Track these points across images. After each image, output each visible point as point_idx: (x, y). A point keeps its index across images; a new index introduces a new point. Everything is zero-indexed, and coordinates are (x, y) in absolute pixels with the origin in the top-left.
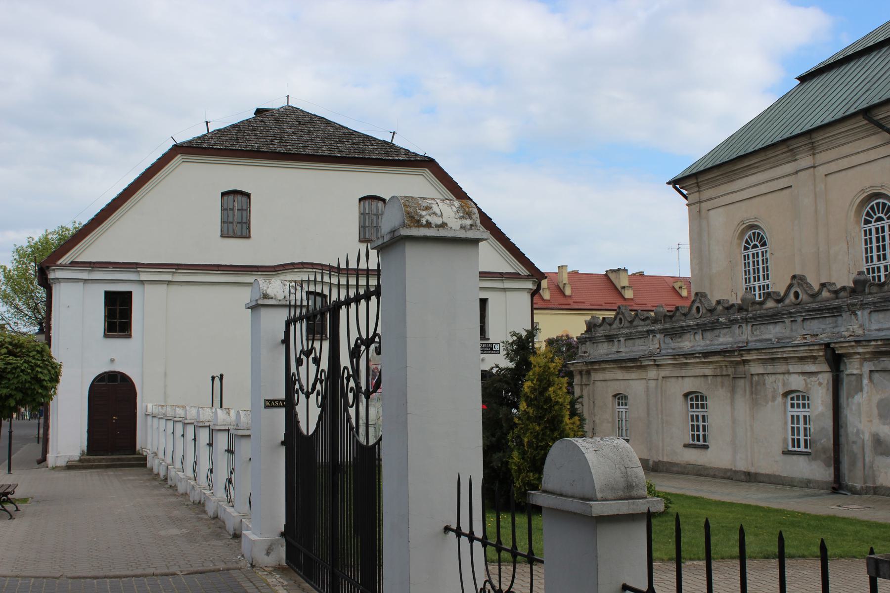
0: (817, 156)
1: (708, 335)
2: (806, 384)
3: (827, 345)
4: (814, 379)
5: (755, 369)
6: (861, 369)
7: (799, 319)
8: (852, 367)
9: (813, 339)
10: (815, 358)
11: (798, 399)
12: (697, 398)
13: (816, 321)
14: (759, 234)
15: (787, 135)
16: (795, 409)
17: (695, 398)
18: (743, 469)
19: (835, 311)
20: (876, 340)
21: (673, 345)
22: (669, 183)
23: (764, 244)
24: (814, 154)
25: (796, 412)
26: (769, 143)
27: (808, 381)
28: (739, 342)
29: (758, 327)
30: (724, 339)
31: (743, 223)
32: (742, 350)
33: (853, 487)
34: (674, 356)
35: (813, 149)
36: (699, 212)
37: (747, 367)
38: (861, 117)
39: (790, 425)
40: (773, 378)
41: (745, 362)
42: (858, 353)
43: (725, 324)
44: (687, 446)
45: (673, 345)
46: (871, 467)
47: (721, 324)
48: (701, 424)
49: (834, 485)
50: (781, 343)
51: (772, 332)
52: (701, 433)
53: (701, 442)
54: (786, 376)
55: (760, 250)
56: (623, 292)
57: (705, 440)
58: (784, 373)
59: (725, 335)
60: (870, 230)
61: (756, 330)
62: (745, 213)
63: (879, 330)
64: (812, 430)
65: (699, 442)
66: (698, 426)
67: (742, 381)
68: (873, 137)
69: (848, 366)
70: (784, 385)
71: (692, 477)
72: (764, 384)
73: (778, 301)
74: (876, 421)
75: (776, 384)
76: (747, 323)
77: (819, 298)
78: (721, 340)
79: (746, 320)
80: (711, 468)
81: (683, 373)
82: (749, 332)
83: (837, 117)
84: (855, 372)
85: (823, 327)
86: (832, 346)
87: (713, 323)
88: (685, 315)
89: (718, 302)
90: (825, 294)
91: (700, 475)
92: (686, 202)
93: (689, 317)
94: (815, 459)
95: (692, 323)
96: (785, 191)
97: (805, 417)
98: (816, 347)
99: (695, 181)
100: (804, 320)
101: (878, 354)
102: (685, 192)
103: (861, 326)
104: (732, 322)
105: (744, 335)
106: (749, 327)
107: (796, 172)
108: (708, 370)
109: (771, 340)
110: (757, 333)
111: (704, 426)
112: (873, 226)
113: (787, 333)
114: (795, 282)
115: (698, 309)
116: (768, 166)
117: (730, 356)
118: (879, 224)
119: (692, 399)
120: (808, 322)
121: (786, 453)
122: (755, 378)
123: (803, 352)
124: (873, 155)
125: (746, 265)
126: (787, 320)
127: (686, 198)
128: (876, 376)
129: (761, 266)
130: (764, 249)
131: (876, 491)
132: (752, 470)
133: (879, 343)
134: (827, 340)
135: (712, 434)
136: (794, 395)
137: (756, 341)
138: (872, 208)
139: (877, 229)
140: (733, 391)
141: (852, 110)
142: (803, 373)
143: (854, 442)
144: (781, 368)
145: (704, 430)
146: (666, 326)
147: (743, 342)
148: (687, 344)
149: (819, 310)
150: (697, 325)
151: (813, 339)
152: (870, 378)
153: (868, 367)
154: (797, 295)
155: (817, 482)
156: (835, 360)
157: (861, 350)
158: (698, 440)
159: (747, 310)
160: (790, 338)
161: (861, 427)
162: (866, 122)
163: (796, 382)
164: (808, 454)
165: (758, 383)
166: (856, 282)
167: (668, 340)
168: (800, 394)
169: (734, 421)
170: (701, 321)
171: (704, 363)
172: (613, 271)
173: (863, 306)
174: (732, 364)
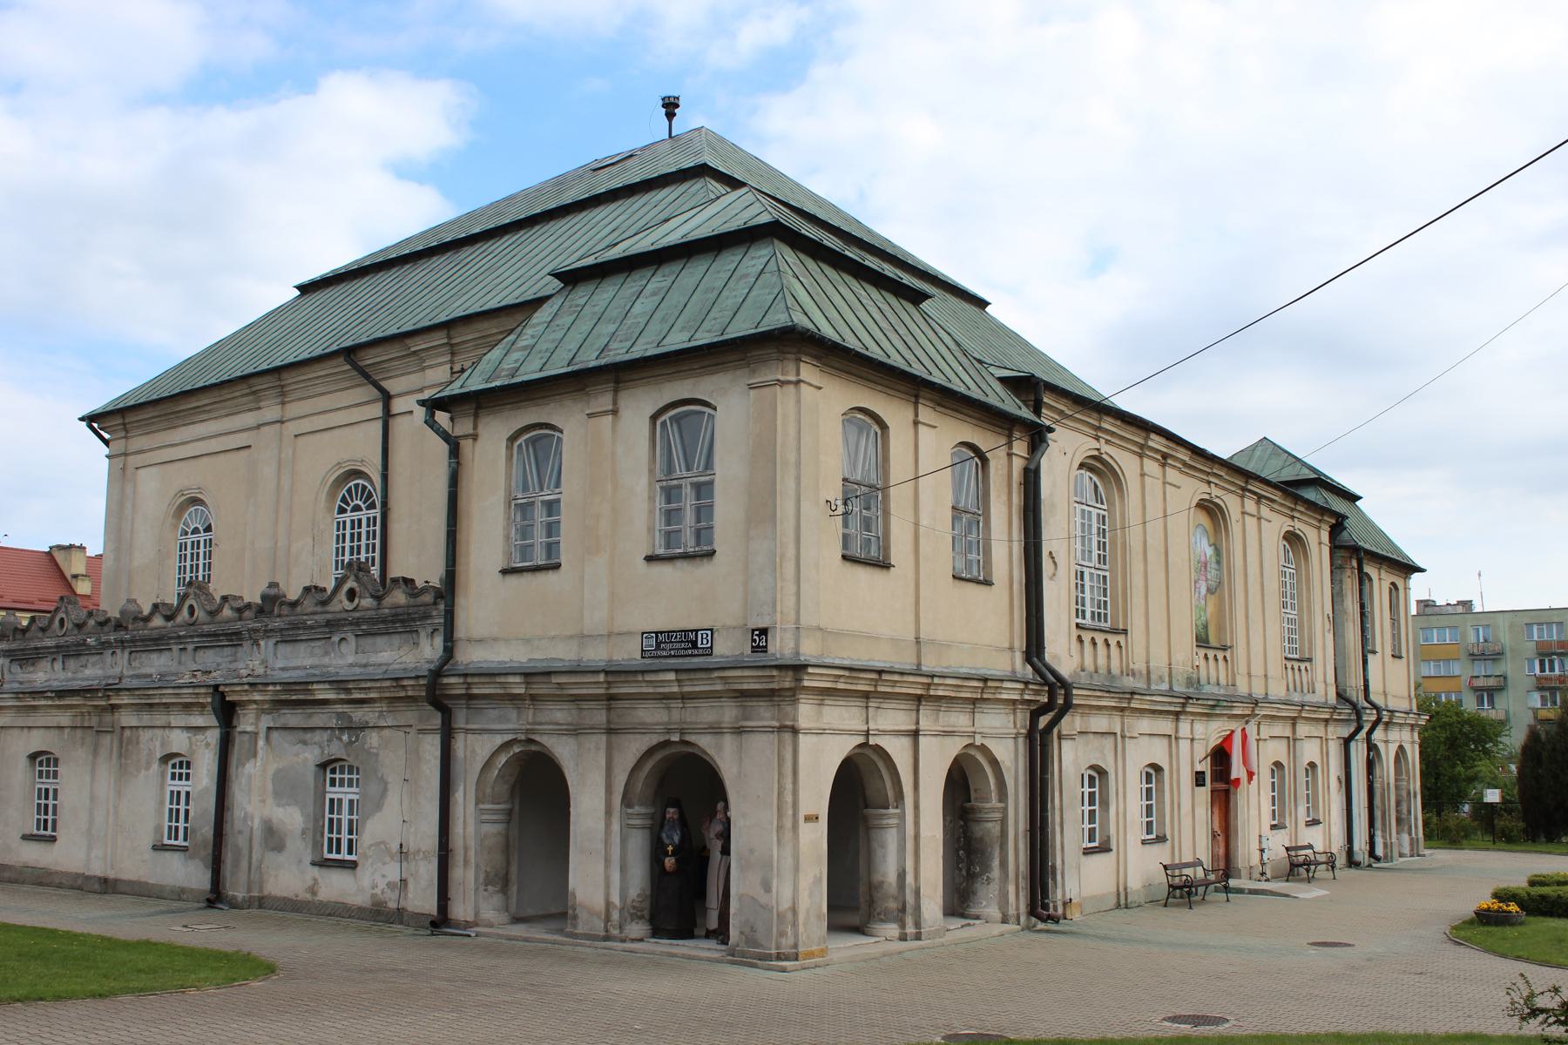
1: (72, 663)
3: (216, 687)
4: (200, 737)
6: (256, 725)
7: (190, 647)
8: (246, 722)
10: (203, 706)
12: (48, 760)
13: (210, 653)
15: (251, 370)
16: (177, 782)
17: (42, 760)
18: (99, 873)
19: (234, 638)
20: (274, 684)
21: (22, 676)
22: (82, 419)
23: (208, 529)
24: (283, 403)
26: (225, 378)
30: (91, 672)
31: (181, 493)
32: (109, 690)
33: (234, 897)
34: (18, 694)
35: (283, 395)
36: (124, 469)
38: (341, 360)
39: (168, 806)
41: (114, 708)
42: (255, 702)
44: (27, 838)
45: (22, 676)
46: (259, 867)
47: (89, 647)
48: (51, 802)
49: (212, 896)
50: (163, 682)
51: (155, 664)
52: (50, 817)
53: (49, 832)
55: (202, 537)
56: (73, 583)
57: (54, 829)
59: (94, 665)
62: (187, 478)
63: (282, 669)
64: (191, 814)
65: (45, 835)
66: (46, 806)
67: (108, 737)
68: (358, 390)
70: (163, 745)
71: (26, 888)
73: (168, 618)
74: (270, 801)
75: (152, 744)
76: (124, 648)
77: (218, 618)
78: (88, 672)
79: (122, 643)
80: (57, 872)
81: (30, 721)
83: (314, 354)
84: (249, 729)
85: (219, 660)
86: (221, 689)
87: (78, 645)
88: (43, 630)
90: (227, 612)
91: (41, 884)
92: (106, 450)
93: (48, 633)
94: (192, 857)
95: (49, 643)
97: (188, 794)
98: (203, 690)
99: (120, 421)
100: (196, 649)
101: (279, 704)
102: (107, 436)
103: (264, 662)
104: (105, 645)
106: (126, 655)
107: (259, 426)
108: (64, 719)
111: (55, 806)
112: (348, 517)
113: (174, 667)
114: (191, 591)
115: (62, 620)
116: (223, 412)
117: (91, 699)
119: (41, 764)
120: (201, 653)
121: (159, 848)
122: (127, 733)
123: (187, 696)
125: (183, 558)
126: (175, 648)
127: (106, 442)
128: (275, 735)
129: (201, 562)
130: (208, 536)
131: (262, 902)
132: (111, 875)
134: (220, 680)
135: (64, 817)
136: (177, 760)
137: (132, 677)
138: (349, 491)
140: (95, 753)
141: (334, 347)
142: (188, 728)
143: (240, 832)
144: (160, 719)
145: (55, 813)
146: (14, 646)
148: (43, 675)
150: (57, 647)
151: (205, 678)
152: (267, 739)
153: (266, 721)
154: (192, 610)
155: (192, 890)
156: (227, 712)
157: (257, 697)
158: (46, 829)
159: (126, 629)
160: (176, 674)
161: (249, 809)
163: (178, 741)
164: (184, 849)
166: (264, 597)
167: (16, 668)
169: (93, 798)
170: (62, 641)
171: (59, 707)
172: (60, 548)
173: (268, 633)
174: (97, 708)
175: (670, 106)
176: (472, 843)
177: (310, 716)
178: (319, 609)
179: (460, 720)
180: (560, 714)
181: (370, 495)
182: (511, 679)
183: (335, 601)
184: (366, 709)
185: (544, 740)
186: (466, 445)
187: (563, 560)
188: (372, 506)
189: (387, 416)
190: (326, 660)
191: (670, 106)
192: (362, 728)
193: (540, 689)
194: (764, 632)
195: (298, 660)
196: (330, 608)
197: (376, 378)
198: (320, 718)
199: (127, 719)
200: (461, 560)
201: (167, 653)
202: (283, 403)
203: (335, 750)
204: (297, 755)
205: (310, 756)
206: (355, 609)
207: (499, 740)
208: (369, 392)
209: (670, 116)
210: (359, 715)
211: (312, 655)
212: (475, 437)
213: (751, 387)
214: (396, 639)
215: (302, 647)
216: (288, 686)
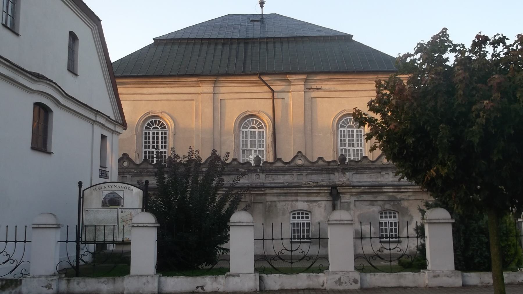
0: (216, 88)
2: (309, 207)
4: (315, 204)
5: (269, 198)
8: (346, 198)
9: (316, 184)
11: (298, 214)
20: (365, 186)
27: (311, 205)
28: (257, 183)
29: (270, 176)
31: (148, 113)
37: (263, 197)
40: (284, 203)
50: (290, 186)
54: (294, 202)
55: (160, 131)
58: (292, 201)
60: (246, 132)
61: (268, 177)
62: (157, 108)
63: (359, 182)
67: (260, 205)
68: (255, 87)
69: (342, 198)
70: (292, 207)
72: (276, 206)
77: (317, 164)
79: (263, 171)
84: (346, 201)
96: (187, 101)
98: (325, 188)
105: (262, 179)
109: (283, 183)
110: (270, 179)
113: (295, 180)
116: (177, 85)
120: (310, 176)
124: (255, 96)
126: (295, 174)
128: (357, 203)
130: (164, 131)
133: (367, 188)
136: (296, 212)
137: (270, 183)
139: (251, 132)
142: (307, 201)
147: (260, 183)
149: (318, 170)
153: (353, 199)
160: (298, 183)
162: (259, 79)
163: (301, 205)
165: (270, 206)
168: (301, 212)
175: (262, 4)
177: (376, 197)
178: (370, 164)
181: (260, 123)
184: (403, 194)
188: (262, 127)
189: (273, 98)
190: (379, 180)
191: (262, 4)
192: (400, 200)
195: (366, 179)
196: (375, 163)
197: (269, 84)
198: (381, 197)
199: (269, 198)
202: (214, 87)
203: (387, 206)
204: (370, 209)
205: (376, 209)
208: (266, 89)
209: (262, 7)
210: (399, 196)
211: (370, 178)
215: (365, 175)
216: (372, 186)
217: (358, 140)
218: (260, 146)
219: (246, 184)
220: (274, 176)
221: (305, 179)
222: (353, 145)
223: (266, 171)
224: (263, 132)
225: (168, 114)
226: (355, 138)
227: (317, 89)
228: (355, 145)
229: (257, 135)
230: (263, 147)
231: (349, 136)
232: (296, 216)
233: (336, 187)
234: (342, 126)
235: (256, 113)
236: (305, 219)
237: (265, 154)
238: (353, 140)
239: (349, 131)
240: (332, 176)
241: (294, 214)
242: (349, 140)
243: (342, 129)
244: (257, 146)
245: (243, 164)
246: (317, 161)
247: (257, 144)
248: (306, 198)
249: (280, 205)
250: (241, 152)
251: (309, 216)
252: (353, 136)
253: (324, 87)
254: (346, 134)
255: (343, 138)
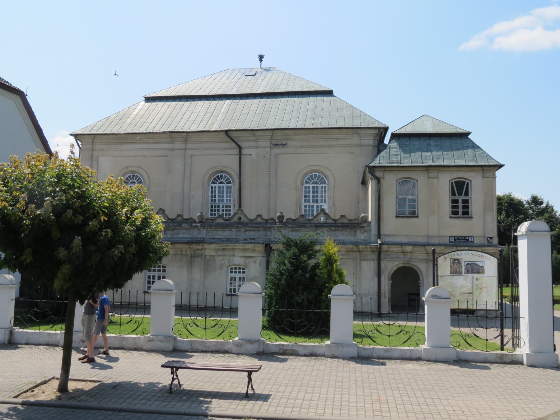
2: (246, 262)
3: (269, 244)
4: (251, 260)
14: (137, 176)
22: (71, 135)
24: (186, 144)
25: (233, 275)
27: (247, 260)
31: (127, 167)
36: (92, 156)
37: (203, 251)
40: (222, 258)
43: (186, 228)
50: (229, 240)
58: (230, 256)
59: (183, 233)
61: (209, 233)
67: (200, 259)
72: (214, 260)
82: (204, 234)
89: (179, 216)
105: (203, 234)
107: (173, 150)
109: (222, 239)
110: (210, 234)
112: (217, 185)
113: (234, 236)
118: (221, 185)
120: (248, 232)
126: (234, 230)
137: (210, 238)
139: (219, 188)
142: (244, 257)
144: (230, 253)
147: (201, 238)
151: (252, 241)
154: (240, 218)
160: (236, 239)
163: (238, 261)
175: (261, 57)
176: (387, 291)
179: (382, 256)
180: (420, 256)
182: (408, 247)
183: (315, 220)
185: (414, 263)
186: (382, 180)
187: (419, 215)
188: (230, 183)
191: (261, 57)
193: (418, 249)
194: (491, 238)
196: (311, 222)
200: (381, 213)
201: (228, 232)
202: (186, 144)
206: (325, 223)
207: (396, 263)
209: (261, 61)
212: (384, 178)
213: (484, 178)
214: (345, 233)
217: (322, 196)
218: (227, 200)
219: (188, 238)
220: (214, 232)
221: (243, 234)
222: (317, 201)
223: (207, 226)
224: (231, 187)
225: (144, 170)
226: (319, 194)
227: (283, 145)
228: (319, 201)
229: (225, 190)
230: (230, 201)
231: (313, 192)
232: (234, 270)
233: (269, 244)
234: (307, 182)
235: (224, 169)
236: (242, 274)
237: (232, 209)
238: (317, 196)
239: (313, 188)
240: (269, 233)
241: (232, 269)
242: (313, 196)
243: (307, 185)
244: (225, 200)
245: (186, 220)
246: (256, 219)
247: (225, 198)
248: (242, 254)
249: (218, 260)
250: (210, 206)
251: (246, 271)
252: (317, 192)
253: (290, 143)
254: (311, 190)
255: (307, 194)
